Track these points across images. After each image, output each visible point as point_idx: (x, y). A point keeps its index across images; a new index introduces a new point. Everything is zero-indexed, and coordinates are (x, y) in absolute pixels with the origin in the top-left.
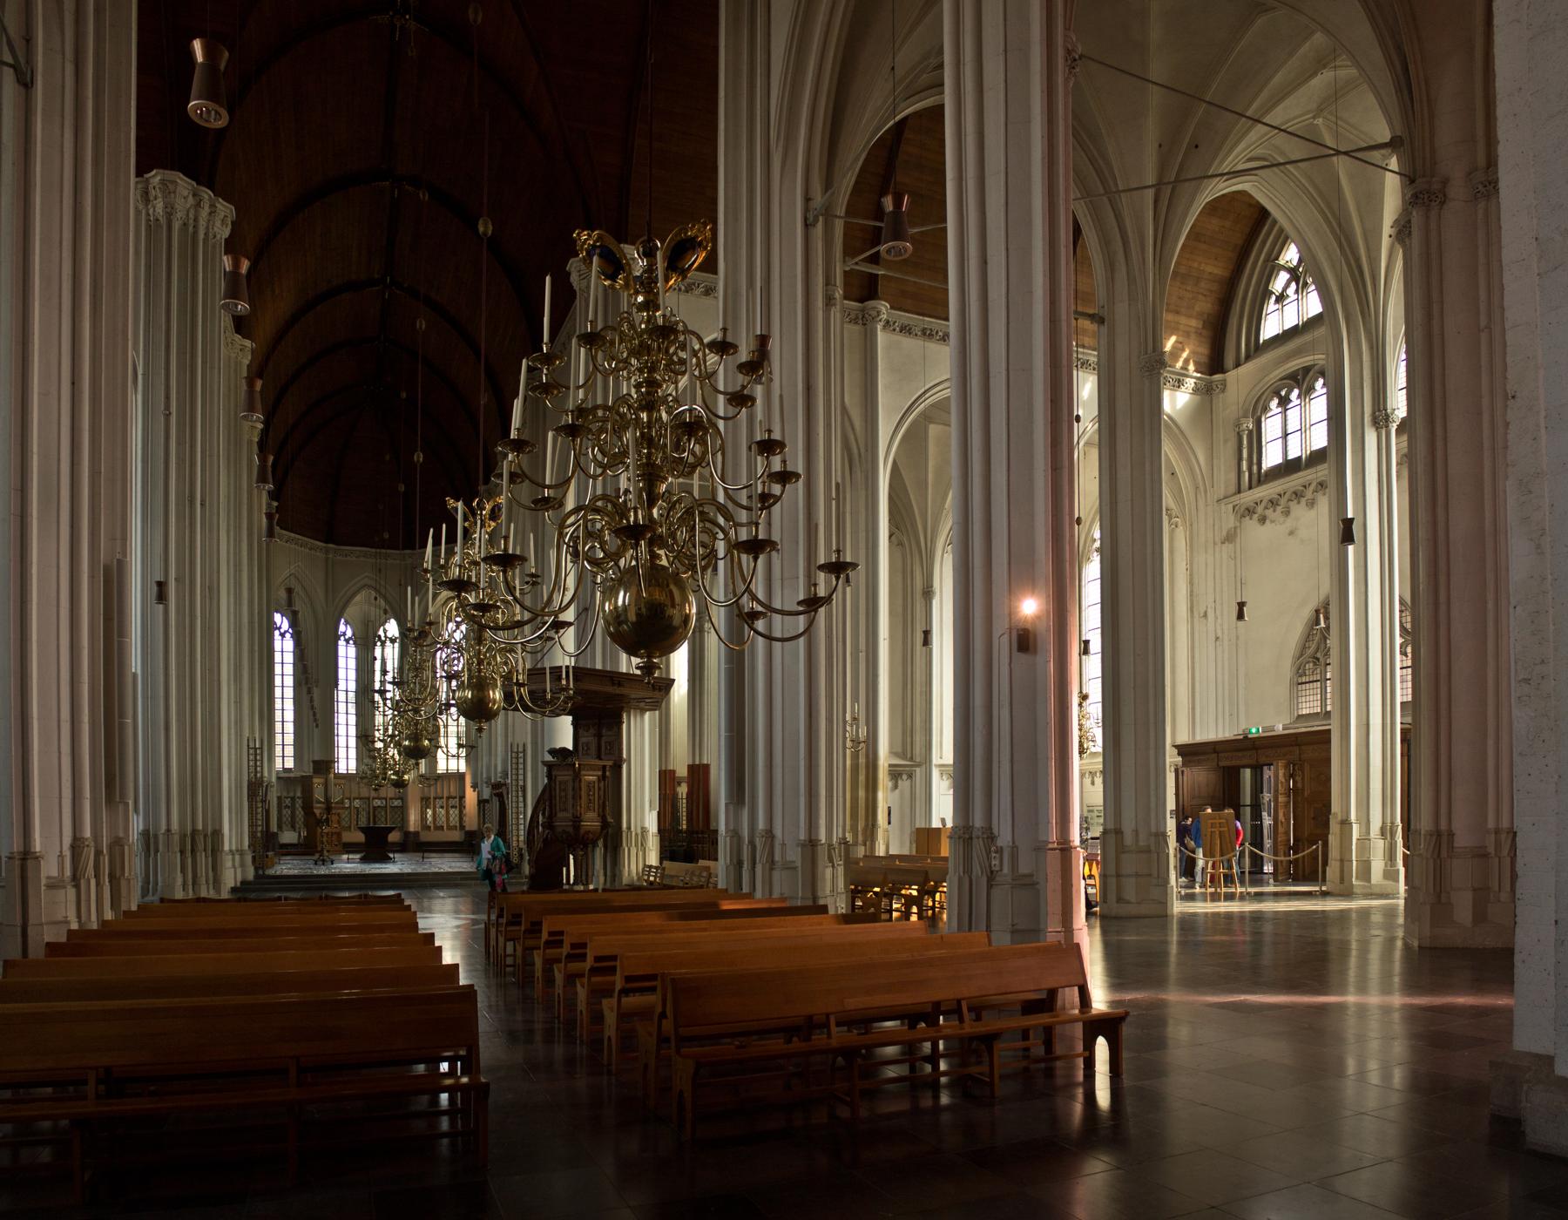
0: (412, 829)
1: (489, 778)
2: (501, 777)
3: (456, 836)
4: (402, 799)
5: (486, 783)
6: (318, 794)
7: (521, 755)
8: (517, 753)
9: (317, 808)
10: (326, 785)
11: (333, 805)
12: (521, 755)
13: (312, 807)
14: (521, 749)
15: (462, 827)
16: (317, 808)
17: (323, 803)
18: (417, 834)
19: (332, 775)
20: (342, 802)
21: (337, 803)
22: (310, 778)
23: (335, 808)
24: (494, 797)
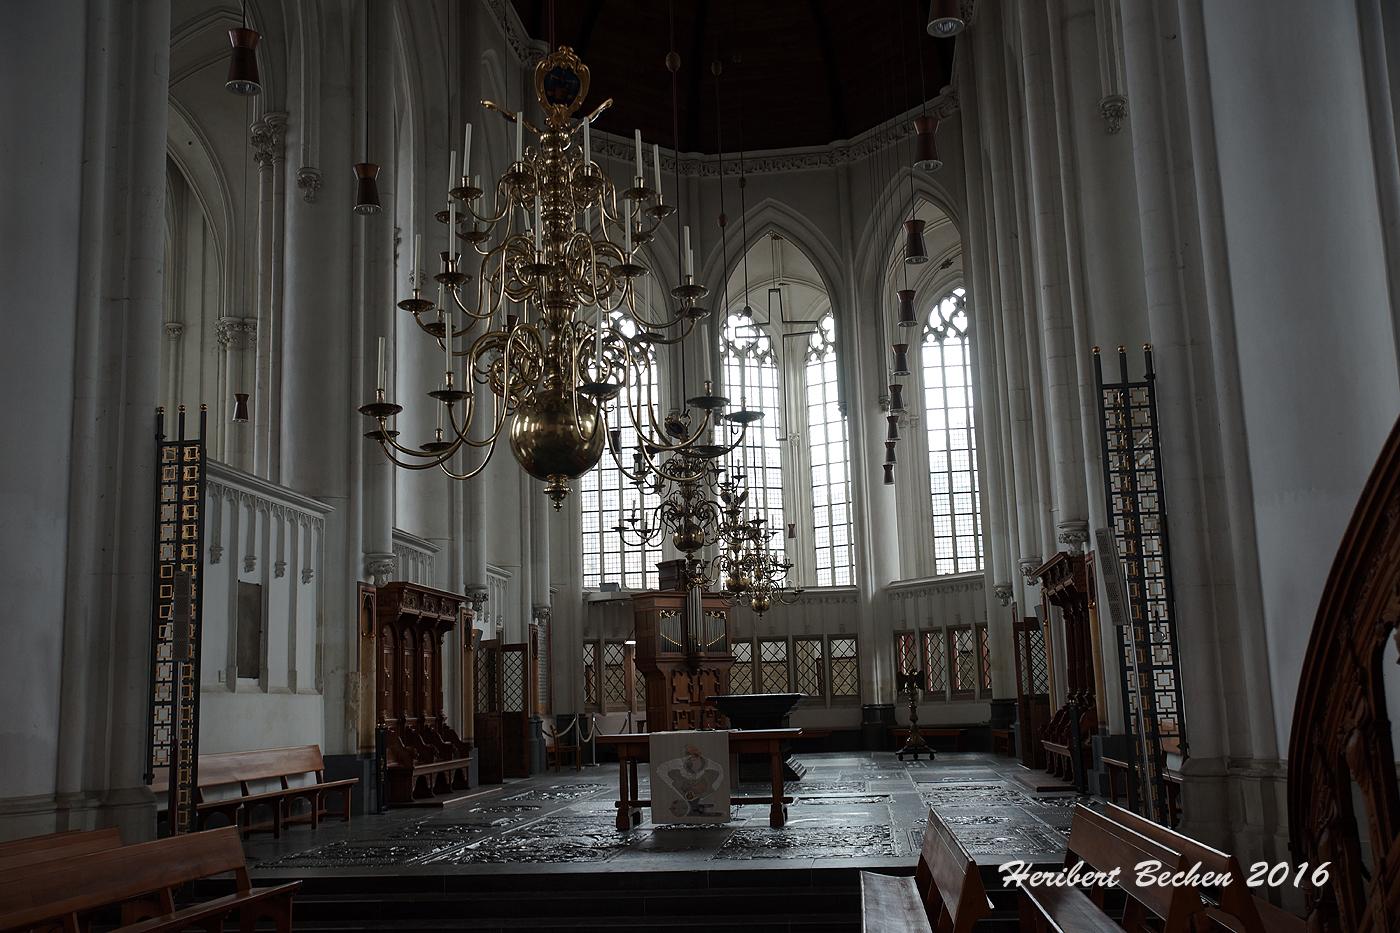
0: (878, 701)
1: (1034, 559)
2: (1066, 539)
3: (979, 713)
4: (854, 637)
5: (1028, 572)
6: (668, 630)
7: (1141, 396)
8: (1124, 387)
9: (665, 661)
10: (684, 613)
11: (702, 654)
12: (1141, 396)
13: (654, 661)
14: (1137, 374)
15: (985, 693)
16: (665, 661)
17: (676, 649)
18: (888, 710)
19: (698, 592)
20: (724, 646)
21: (710, 649)
22: (651, 594)
23: (710, 660)
24: (1051, 607)
